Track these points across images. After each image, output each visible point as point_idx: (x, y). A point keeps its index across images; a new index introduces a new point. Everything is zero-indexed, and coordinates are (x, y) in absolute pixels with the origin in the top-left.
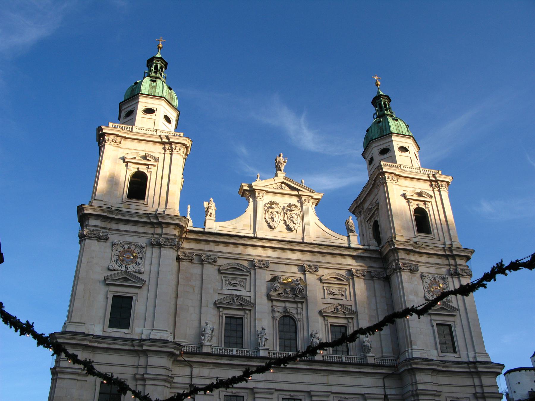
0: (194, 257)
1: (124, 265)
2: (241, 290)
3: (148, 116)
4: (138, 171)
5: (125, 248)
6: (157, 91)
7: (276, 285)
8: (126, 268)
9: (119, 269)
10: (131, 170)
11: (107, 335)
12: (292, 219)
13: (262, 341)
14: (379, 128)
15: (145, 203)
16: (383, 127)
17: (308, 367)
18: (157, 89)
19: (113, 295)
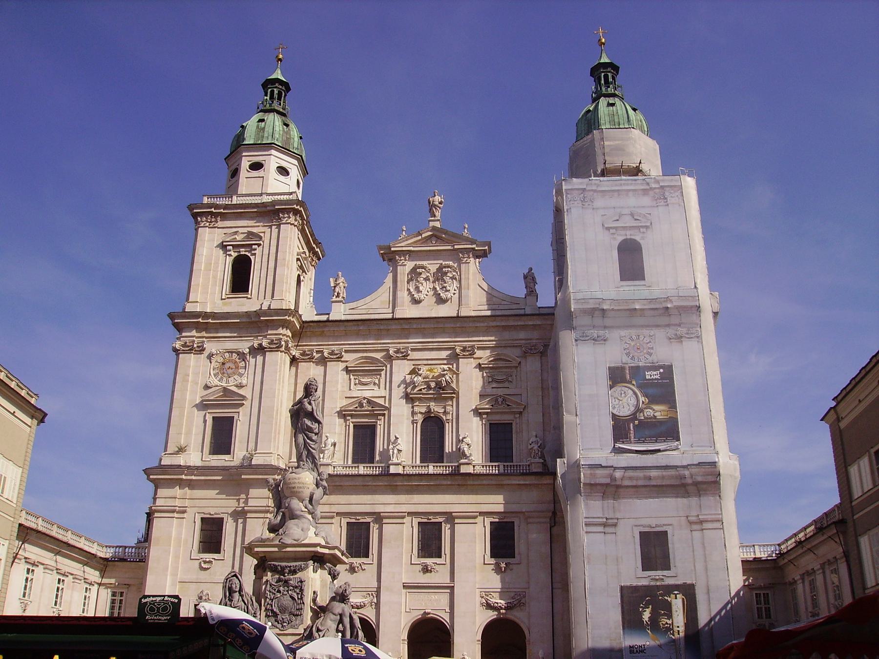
0: (315, 354)
1: (225, 379)
2: (373, 390)
3: (255, 173)
4: (238, 256)
5: (226, 357)
6: (266, 135)
7: (415, 379)
8: (228, 382)
9: (218, 385)
10: (232, 256)
11: (207, 464)
12: (445, 285)
13: (393, 452)
14: (587, 122)
15: (249, 296)
16: (591, 119)
17: (449, 483)
18: (265, 133)
19: (213, 417)
